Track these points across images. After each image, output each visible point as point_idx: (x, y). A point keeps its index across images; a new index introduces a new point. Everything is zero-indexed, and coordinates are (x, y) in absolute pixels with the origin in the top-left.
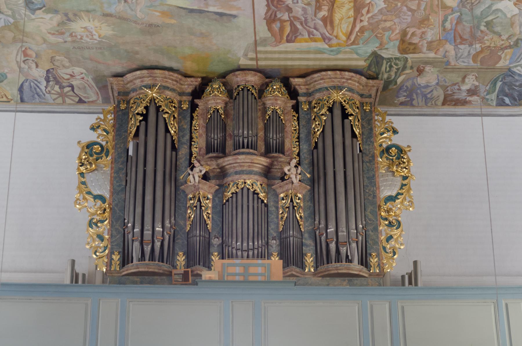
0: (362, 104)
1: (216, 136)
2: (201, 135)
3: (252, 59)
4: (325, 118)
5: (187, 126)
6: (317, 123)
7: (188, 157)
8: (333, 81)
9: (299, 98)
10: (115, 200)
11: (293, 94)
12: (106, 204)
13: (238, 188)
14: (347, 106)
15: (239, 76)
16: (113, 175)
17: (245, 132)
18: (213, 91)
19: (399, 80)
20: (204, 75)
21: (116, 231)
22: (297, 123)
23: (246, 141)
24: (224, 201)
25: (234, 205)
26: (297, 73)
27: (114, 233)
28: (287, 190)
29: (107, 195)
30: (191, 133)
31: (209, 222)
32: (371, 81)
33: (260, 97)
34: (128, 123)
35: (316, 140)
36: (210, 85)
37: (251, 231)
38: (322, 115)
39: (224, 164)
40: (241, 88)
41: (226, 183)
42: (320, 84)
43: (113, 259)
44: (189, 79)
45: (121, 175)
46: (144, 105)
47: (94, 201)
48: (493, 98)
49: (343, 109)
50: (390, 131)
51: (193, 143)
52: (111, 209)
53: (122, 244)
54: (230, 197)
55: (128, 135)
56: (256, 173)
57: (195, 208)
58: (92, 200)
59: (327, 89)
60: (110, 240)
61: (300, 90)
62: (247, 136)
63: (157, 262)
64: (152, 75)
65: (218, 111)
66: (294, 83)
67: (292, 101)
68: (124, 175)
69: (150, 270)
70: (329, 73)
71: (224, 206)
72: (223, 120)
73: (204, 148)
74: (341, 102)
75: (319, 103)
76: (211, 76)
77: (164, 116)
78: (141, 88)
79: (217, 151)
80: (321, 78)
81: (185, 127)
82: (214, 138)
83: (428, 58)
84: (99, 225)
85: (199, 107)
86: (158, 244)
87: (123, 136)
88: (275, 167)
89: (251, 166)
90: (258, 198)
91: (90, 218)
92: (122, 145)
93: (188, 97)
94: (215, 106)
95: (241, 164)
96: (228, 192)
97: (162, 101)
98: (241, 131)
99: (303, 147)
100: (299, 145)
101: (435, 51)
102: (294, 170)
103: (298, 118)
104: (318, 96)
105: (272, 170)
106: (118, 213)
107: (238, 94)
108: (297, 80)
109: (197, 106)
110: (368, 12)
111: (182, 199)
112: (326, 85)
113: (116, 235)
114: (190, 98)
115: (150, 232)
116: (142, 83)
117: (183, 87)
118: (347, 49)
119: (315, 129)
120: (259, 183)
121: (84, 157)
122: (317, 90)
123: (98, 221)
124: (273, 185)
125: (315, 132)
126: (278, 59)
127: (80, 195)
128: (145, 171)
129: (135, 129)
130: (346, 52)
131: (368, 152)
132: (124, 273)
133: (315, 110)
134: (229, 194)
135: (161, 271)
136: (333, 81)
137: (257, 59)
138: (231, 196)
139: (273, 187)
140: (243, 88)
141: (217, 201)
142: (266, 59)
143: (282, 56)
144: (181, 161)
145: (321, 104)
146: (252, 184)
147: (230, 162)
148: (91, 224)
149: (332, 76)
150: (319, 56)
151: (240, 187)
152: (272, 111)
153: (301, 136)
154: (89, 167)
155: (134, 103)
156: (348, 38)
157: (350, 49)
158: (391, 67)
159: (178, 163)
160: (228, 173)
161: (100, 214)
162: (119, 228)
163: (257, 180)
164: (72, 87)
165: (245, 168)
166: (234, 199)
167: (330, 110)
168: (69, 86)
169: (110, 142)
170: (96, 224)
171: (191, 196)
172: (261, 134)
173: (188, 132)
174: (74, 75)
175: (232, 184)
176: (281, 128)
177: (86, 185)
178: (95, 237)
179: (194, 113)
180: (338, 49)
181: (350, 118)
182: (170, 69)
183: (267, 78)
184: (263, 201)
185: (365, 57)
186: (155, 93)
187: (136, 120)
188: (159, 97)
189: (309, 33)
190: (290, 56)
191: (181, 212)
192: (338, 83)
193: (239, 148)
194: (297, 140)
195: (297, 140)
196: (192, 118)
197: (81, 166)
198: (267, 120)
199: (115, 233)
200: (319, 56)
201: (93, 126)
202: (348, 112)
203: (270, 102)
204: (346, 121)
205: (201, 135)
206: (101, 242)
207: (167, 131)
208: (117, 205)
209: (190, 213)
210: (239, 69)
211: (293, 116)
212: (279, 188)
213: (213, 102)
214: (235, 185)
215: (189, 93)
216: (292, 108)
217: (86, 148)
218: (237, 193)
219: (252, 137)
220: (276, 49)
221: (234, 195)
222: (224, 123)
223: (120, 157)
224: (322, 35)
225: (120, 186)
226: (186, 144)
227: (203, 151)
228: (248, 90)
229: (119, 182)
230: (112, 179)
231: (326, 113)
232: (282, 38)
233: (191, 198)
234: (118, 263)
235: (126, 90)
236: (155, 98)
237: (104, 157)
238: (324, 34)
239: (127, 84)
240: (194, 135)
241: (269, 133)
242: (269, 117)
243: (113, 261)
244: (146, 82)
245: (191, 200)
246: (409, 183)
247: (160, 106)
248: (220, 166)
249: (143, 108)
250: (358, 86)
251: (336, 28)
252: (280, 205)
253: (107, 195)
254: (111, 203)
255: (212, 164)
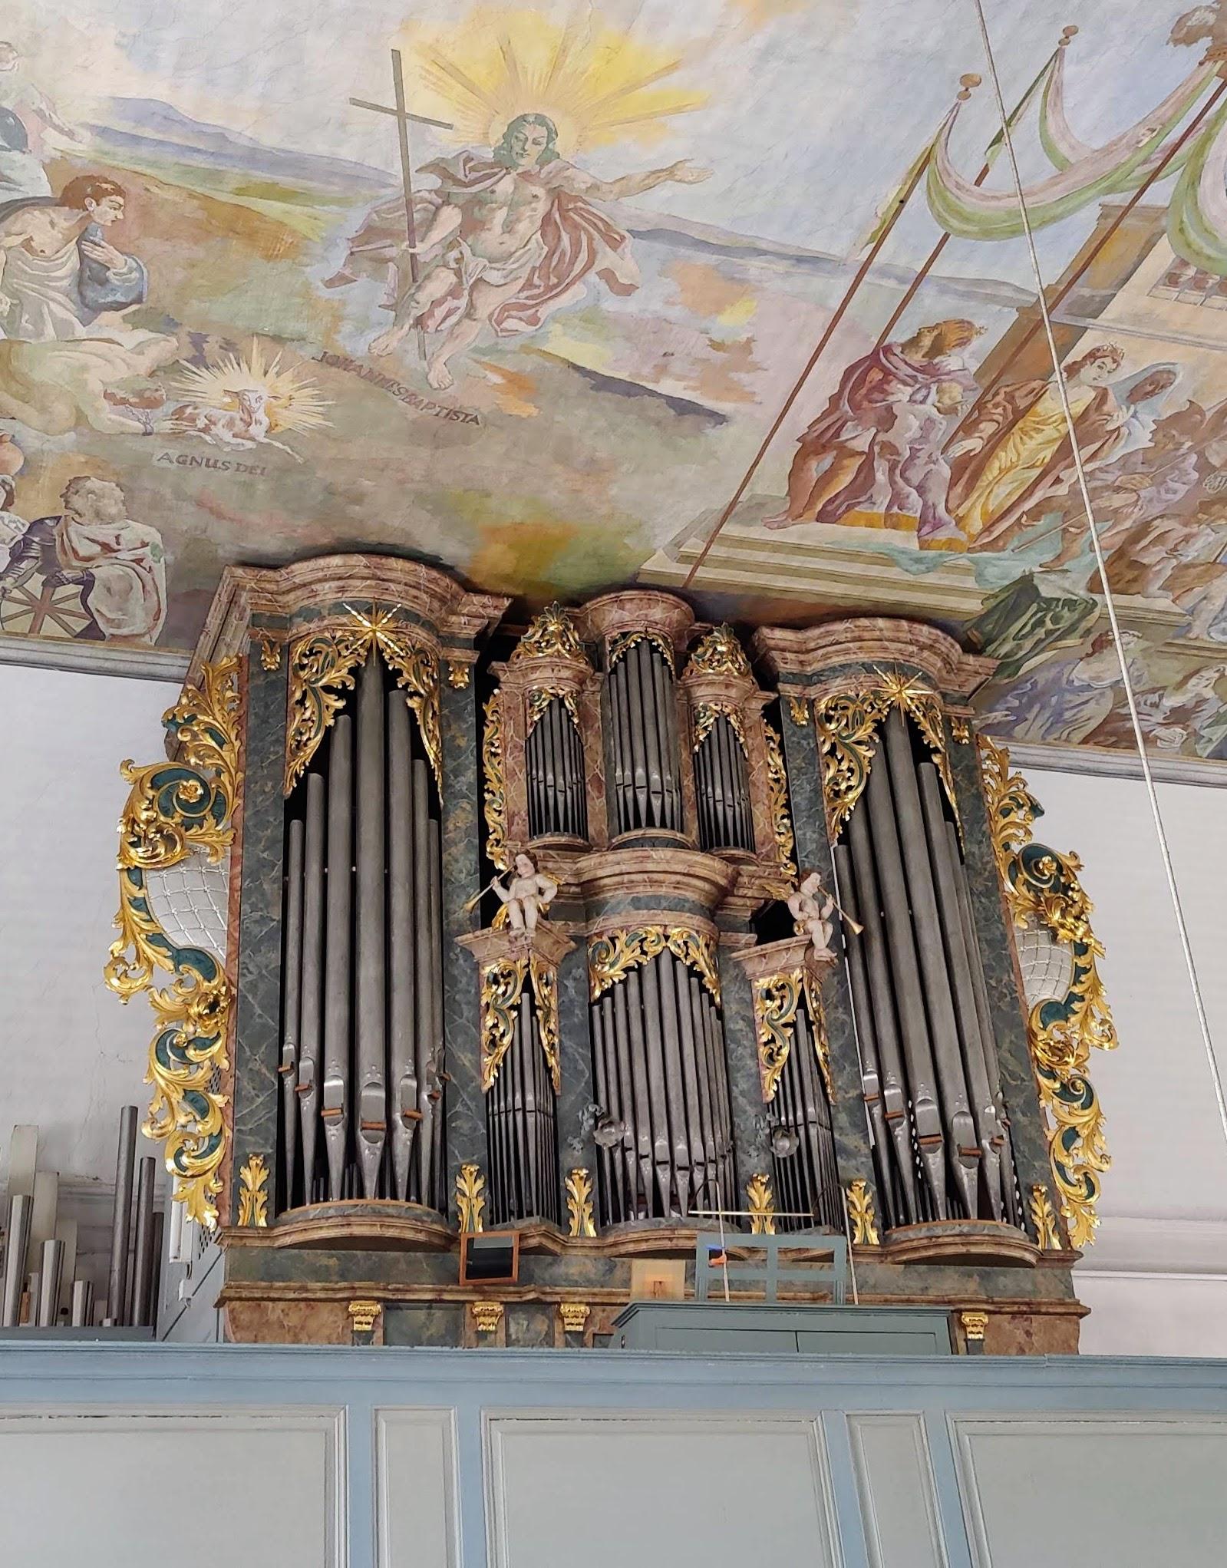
0: (947, 720)
1: (560, 781)
2: (511, 774)
3: (685, 559)
4: (870, 754)
5: (467, 742)
6: (844, 766)
7: (476, 841)
8: (886, 649)
9: (780, 686)
10: (250, 973)
11: (764, 674)
12: (215, 982)
13: (644, 953)
14: (925, 725)
15: (628, 606)
16: (238, 882)
17: (655, 776)
18: (548, 641)
19: (1027, 667)
20: (519, 592)
21: (253, 1081)
22: (779, 761)
23: (656, 803)
24: (597, 993)
25: (635, 1011)
26: (781, 614)
27: (247, 1087)
28: (786, 969)
29: (220, 953)
30: (480, 764)
31: (552, 1061)
32: (971, 659)
33: (679, 675)
34: (287, 715)
35: (847, 818)
36: (537, 624)
37: (693, 1100)
38: (859, 743)
39: (600, 873)
40: (635, 642)
41: (600, 935)
42: (847, 652)
43: (243, 1184)
44: (476, 599)
45: (265, 886)
46: (348, 664)
47: (177, 969)
48: (1214, 739)
49: (915, 733)
50: (1023, 806)
51: (487, 796)
52: (233, 1000)
53: (274, 1129)
54: (620, 981)
55: (288, 754)
56: (678, 906)
57: (515, 1014)
58: (170, 964)
59: (868, 668)
60: (230, 1112)
61: (782, 665)
62: (644, 784)
63: (402, 1201)
64: (379, 573)
65: (562, 704)
66: (772, 643)
67: (767, 693)
68: (276, 886)
69: (391, 1233)
70: (881, 622)
71: (596, 1008)
72: (575, 733)
73: (524, 814)
74: (907, 714)
75: (845, 708)
76: (534, 596)
77: (411, 703)
78: (338, 608)
79: (566, 829)
80: (853, 635)
81: (462, 742)
82: (555, 786)
83: (1148, 610)
84: (191, 1053)
85: (501, 685)
86: (403, 1136)
87: (273, 757)
88: (741, 892)
89: (684, 883)
90: (703, 989)
91: (159, 1027)
92: (270, 784)
93: (469, 653)
94: (553, 688)
95: (655, 876)
96: (612, 965)
97: (402, 658)
98: (640, 772)
99: (804, 834)
100: (792, 826)
101: (1178, 592)
102: (811, 907)
103: (781, 745)
104: (838, 686)
105: (731, 899)
106: (260, 1016)
107: (624, 659)
108: (779, 633)
109: (496, 682)
110: (1093, 457)
111: (464, 980)
112: (863, 657)
113: (253, 1093)
114: (473, 656)
115: (381, 1094)
116: (340, 595)
117: (453, 619)
118: (963, 561)
119: (837, 784)
120: (702, 942)
121: (144, 816)
122: (833, 669)
123: (190, 1042)
124: (734, 950)
125: (837, 794)
126: (761, 568)
127: (125, 946)
128: (354, 880)
129: (319, 737)
130: (953, 569)
131: (980, 865)
132: (288, 1240)
133: (832, 726)
134: (616, 973)
135: (422, 1237)
136: (886, 649)
137: (699, 561)
138: (622, 978)
139: (734, 955)
140: (639, 640)
141: (572, 991)
142: (726, 563)
143: (778, 559)
144: (454, 850)
145: (850, 713)
146: (685, 943)
147: (624, 868)
148: (167, 1049)
149: (887, 634)
150: (875, 571)
151: (653, 949)
152: (716, 720)
153: (796, 799)
154: (161, 850)
155: (311, 654)
156: (988, 529)
157: (968, 559)
158: (1040, 623)
159: (445, 857)
160: (605, 902)
161: (200, 1016)
162: (264, 1070)
163: (697, 932)
164: (87, 583)
165: (662, 891)
166: (633, 990)
167: (881, 729)
168: (77, 582)
169: (230, 772)
170: (180, 1051)
171: (496, 971)
172: (688, 782)
173: (472, 759)
174: (116, 547)
175: (623, 937)
176: (742, 775)
177: (148, 913)
178: (177, 1097)
179: (487, 703)
180: (941, 556)
181: (936, 759)
182: (432, 562)
183: (697, 619)
184: (711, 997)
185: (992, 589)
186: (384, 630)
187: (321, 707)
188: (392, 645)
189: (898, 499)
190: (796, 561)
191: (463, 1021)
192: (897, 656)
193: (638, 825)
194: (785, 812)
195: (785, 812)
196: (481, 719)
197: (132, 844)
198: (702, 746)
199: (249, 1088)
200: (875, 571)
201: (174, 715)
202: (929, 743)
203: (709, 690)
204: (925, 766)
205: (511, 774)
206: (198, 1118)
207: (417, 751)
208: (253, 987)
209: (495, 1026)
210: (634, 584)
211: (768, 738)
212: (757, 960)
213: (548, 673)
214: (636, 943)
215: (468, 640)
216: (764, 716)
217: (149, 785)
218: (639, 969)
219: (662, 793)
220: (776, 536)
221: (633, 975)
222: (579, 740)
223: (263, 825)
224: (925, 506)
225: (263, 921)
226: (465, 797)
227: (521, 825)
228: (654, 649)
229: (261, 910)
230: (237, 895)
231: (871, 737)
232: (810, 504)
233: (495, 975)
234: (262, 1198)
235: (279, 609)
236: (382, 646)
237: (211, 821)
238: (934, 506)
239: (289, 591)
240: (488, 770)
241: (710, 782)
242: (708, 737)
243: (242, 1191)
244: (354, 594)
245: (496, 981)
246: (1092, 963)
247: (398, 673)
248: (586, 877)
249: (346, 670)
250: (939, 670)
251: (975, 495)
252: (760, 1013)
253: (220, 953)
254: (234, 979)
255: (560, 868)
